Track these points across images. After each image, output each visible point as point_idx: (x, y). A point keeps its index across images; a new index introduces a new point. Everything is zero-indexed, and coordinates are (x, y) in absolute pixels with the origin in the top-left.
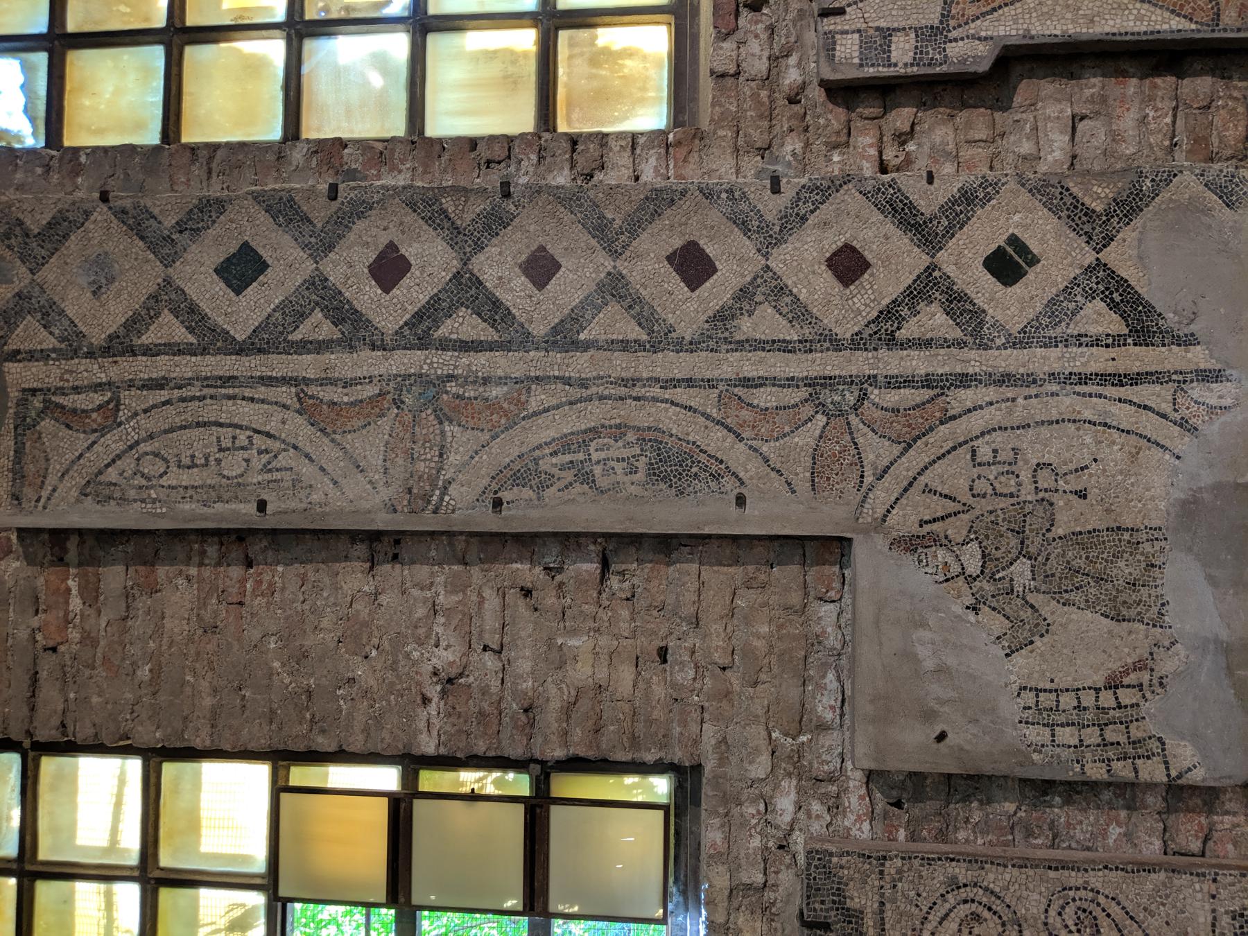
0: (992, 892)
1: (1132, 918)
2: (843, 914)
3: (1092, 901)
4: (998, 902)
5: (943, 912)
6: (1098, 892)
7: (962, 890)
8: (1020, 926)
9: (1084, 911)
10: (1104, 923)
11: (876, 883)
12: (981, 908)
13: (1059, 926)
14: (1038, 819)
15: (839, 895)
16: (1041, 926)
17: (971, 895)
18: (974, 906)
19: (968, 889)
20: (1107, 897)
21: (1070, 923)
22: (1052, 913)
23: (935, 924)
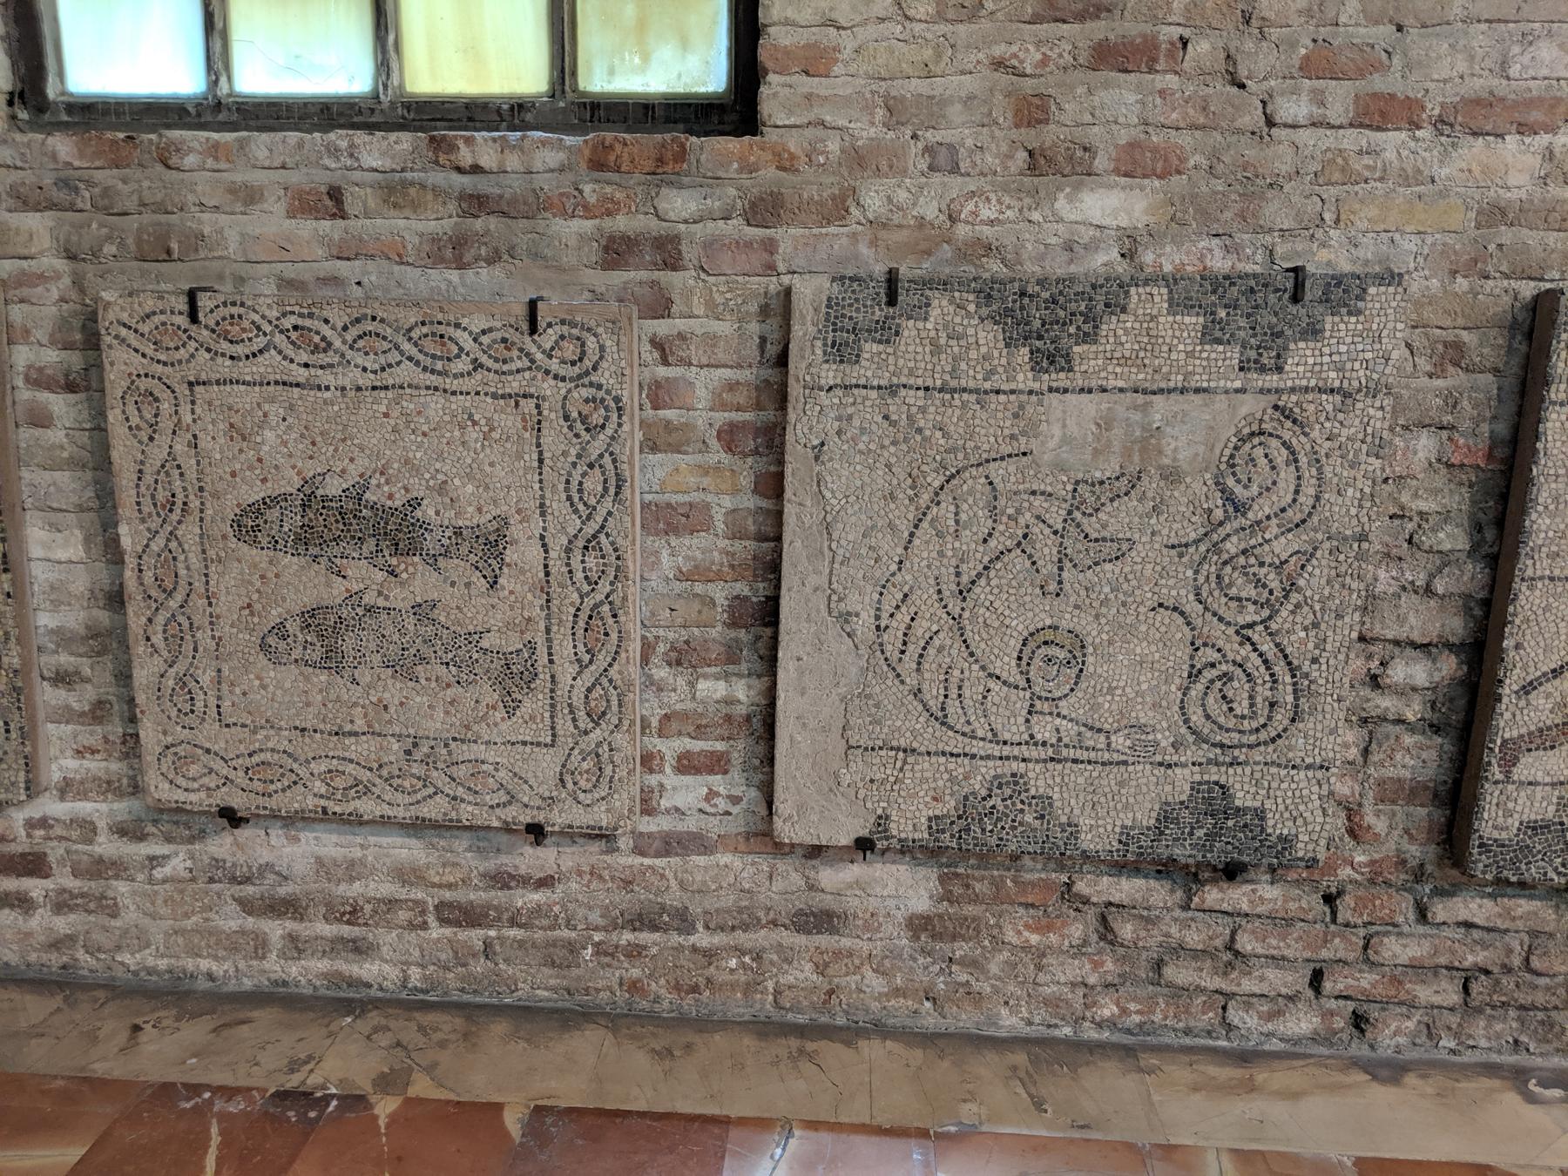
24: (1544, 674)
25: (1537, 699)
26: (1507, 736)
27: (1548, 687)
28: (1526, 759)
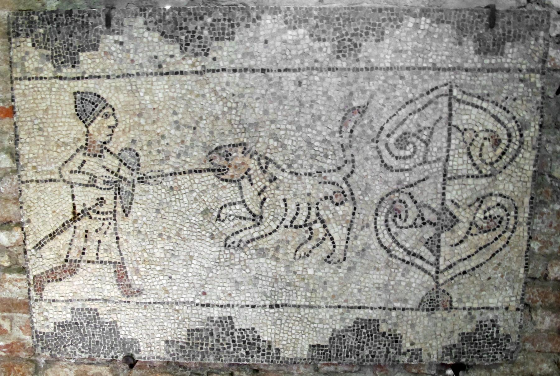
0: (516, 155)
1: (493, 255)
2: (500, 39)
3: (507, 228)
4: (508, 160)
5: (502, 118)
6: (513, 232)
7: (518, 133)
8: (491, 175)
9: (500, 222)
10: (491, 236)
11: (524, 67)
12: (503, 147)
13: (489, 204)
14: (547, 192)
15: (515, 36)
16: (489, 191)
17: (514, 140)
18: (505, 142)
19: (518, 138)
20: (509, 238)
21: (491, 212)
22: (499, 199)
23: (492, 111)
24: (46, 237)
25: (45, 252)
26: (35, 273)
27: (50, 244)
28: (48, 287)
